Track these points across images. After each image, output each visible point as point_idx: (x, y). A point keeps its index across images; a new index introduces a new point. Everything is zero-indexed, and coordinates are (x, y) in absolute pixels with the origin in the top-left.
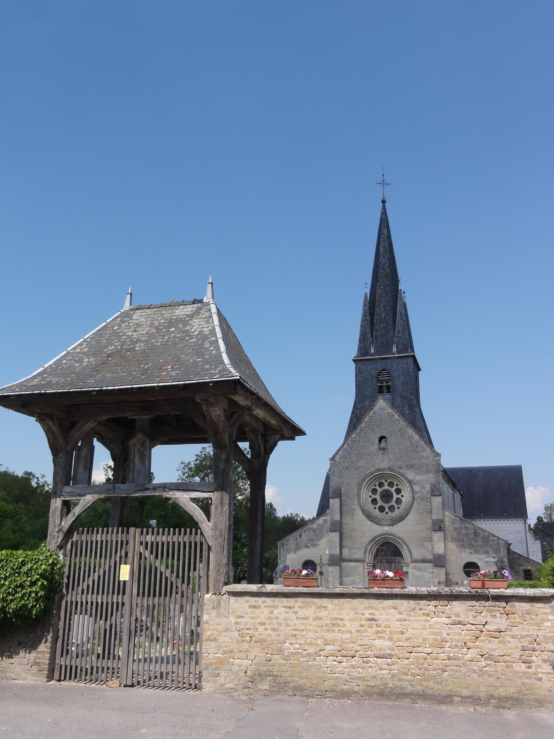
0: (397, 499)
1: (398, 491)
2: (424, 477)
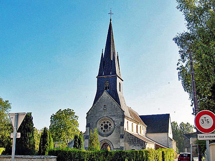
0: (110, 127)
1: (110, 125)
2: (119, 119)
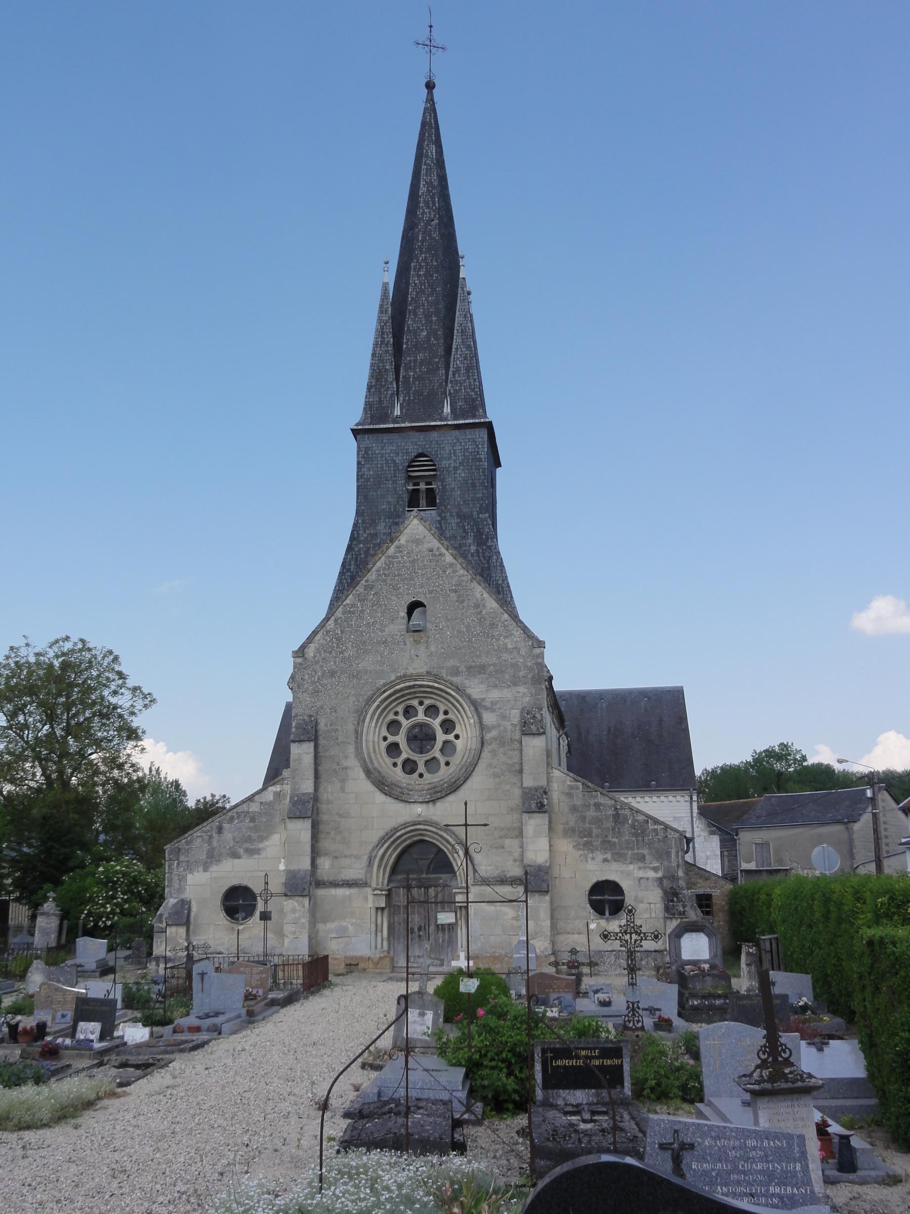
0: (446, 743)
1: (448, 726)
2: (507, 694)
